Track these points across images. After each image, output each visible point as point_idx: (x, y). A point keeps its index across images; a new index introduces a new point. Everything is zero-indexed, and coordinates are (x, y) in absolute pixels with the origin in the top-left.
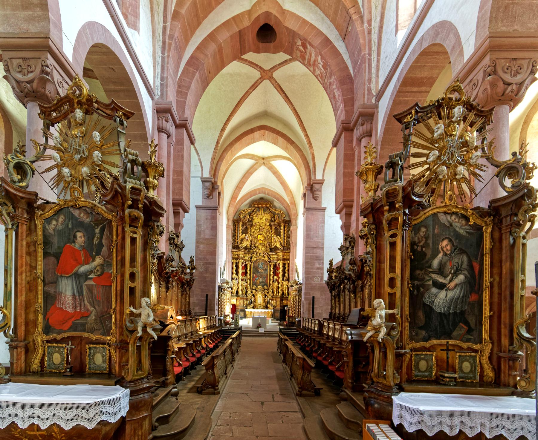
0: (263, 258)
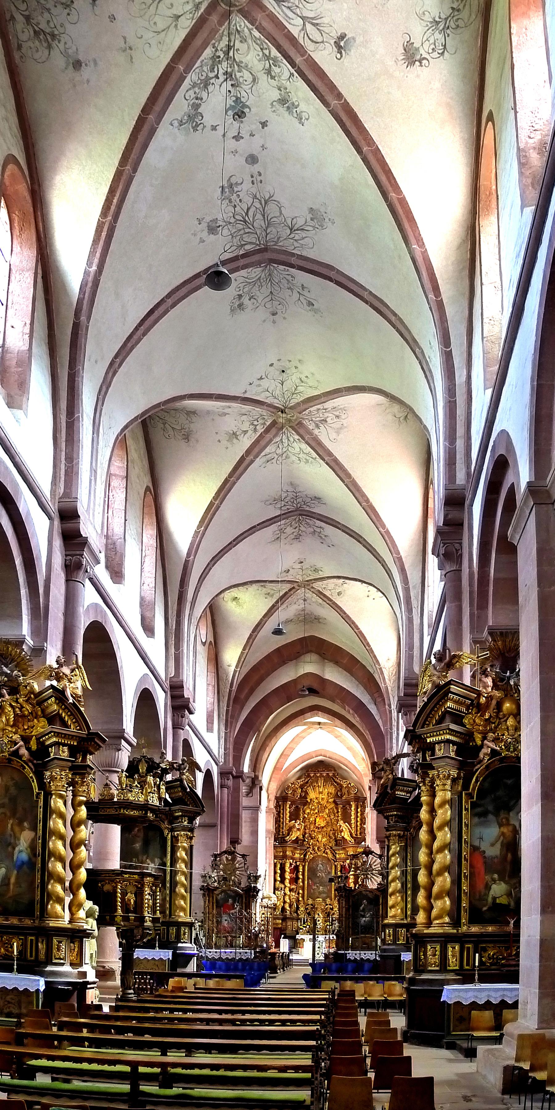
0: (324, 855)
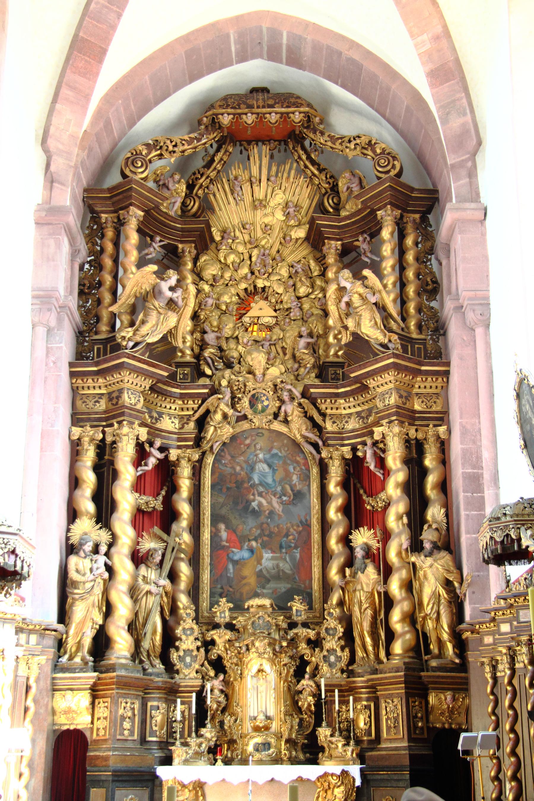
0: (277, 426)
